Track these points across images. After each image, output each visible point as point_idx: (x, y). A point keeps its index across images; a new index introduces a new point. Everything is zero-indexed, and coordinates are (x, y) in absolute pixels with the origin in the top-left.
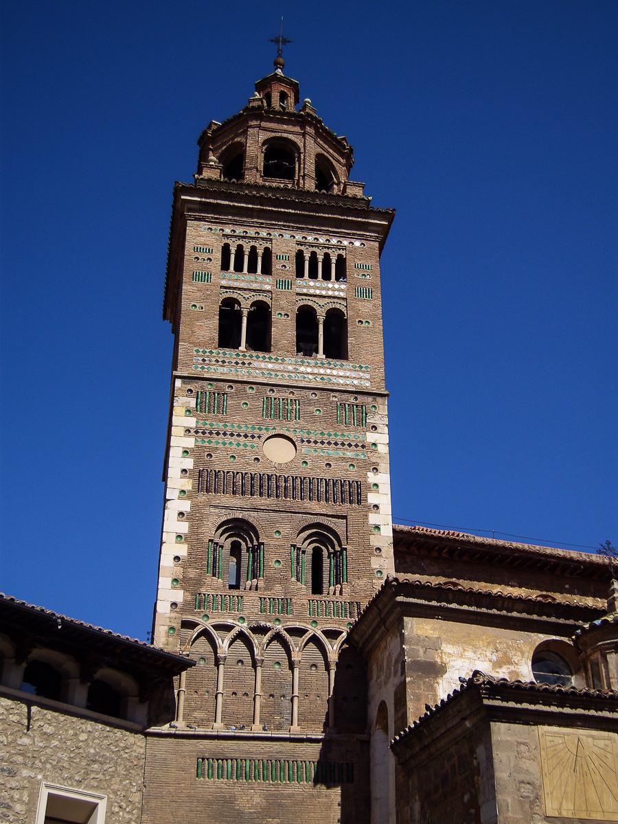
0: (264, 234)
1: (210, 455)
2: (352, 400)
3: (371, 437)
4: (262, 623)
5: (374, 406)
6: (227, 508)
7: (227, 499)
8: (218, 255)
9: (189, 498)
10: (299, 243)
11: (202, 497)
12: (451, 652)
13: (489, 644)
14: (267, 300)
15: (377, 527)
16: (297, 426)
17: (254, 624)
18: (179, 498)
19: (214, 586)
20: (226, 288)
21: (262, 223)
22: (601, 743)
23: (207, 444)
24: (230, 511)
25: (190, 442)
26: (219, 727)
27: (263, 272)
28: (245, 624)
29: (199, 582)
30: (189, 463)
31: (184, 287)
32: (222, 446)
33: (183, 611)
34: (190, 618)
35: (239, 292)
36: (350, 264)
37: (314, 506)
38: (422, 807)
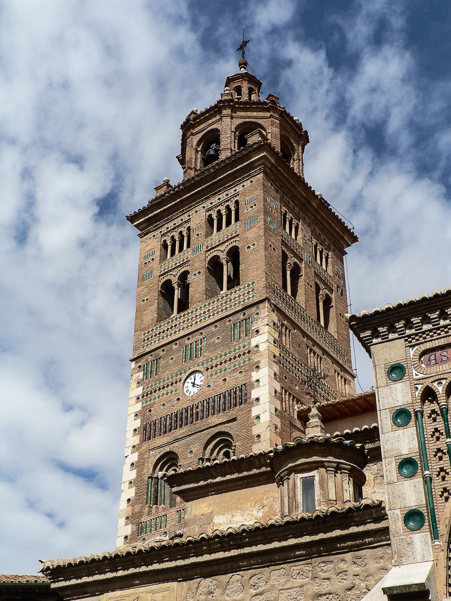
0: (185, 217)
1: (150, 411)
2: (242, 317)
4: (178, 532)
5: (258, 313)
6: (159, 447)
8: (158, 253)
11: (145, 446)
12: (221, 521)
13: (256, 502)
15: (258, 417)
16: (204, 359)
18: (132, 453)
20: (162, 275)
21: (183, 211)
22: (159, 596)
23: (149, 403)
25: (138, 407)
29: (140, 514)
32: (157, 399)
35: (170, 273)
36: (241, 204)
37: (214, 420)
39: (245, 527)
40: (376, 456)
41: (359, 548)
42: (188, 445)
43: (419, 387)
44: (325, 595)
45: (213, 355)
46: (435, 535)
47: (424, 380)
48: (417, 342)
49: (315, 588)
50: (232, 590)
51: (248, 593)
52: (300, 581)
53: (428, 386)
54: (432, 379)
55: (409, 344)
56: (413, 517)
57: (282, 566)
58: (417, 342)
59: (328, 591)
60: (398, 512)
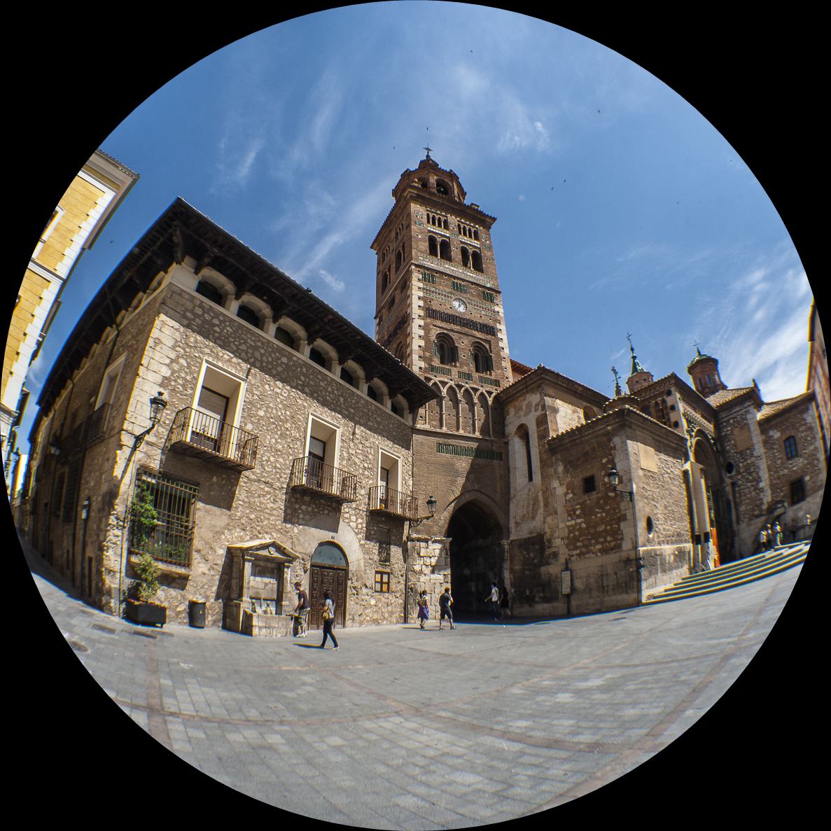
1: (430, 302)
3: (497, 309)
4: (460, 383)
6: (439, 327)
7: (439, 323)
9: (423, 319)
10: (458, 221)
11: (429, 320)
14: (448, 240)
17: (456, 383)
19: (436, 362)
24: (438, 329)
26: (444, 429)
27: (444, 228)
28: (453, 382)
30: (421, 303)
31: (412, 227)
33: (425, 372)
34: (428, 376)
37: (478, 335)
38: (564, 468)
42: (460, 338)
45: (471, 298)
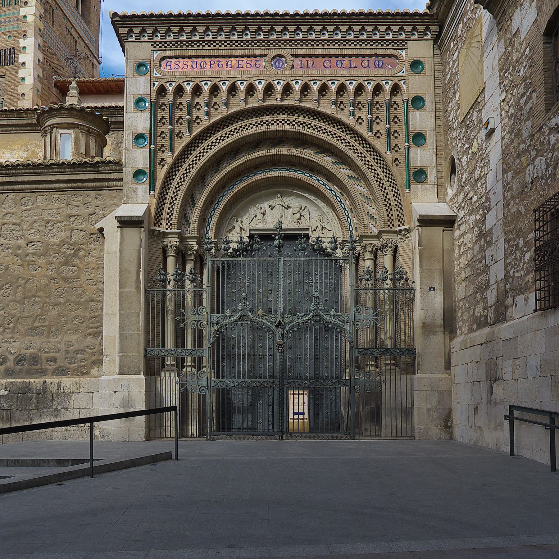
39: (19, 162)
40: (119, 126)
41: (101, 188)
43: (156, 83)
44: (75, 216)
46: (152, 188)
47: (160, 79)
48: (160, 49)
49: (69, 212)
50: (7, 205)
51: (19, 209)
52: (58, 205)
53: (162, 85)
54: (166, 80)
55: (154, 49)
56: (138, 173)
57: (45, 193)
58: (160, 49)
59: (77, 214)
60: (130, 169)
